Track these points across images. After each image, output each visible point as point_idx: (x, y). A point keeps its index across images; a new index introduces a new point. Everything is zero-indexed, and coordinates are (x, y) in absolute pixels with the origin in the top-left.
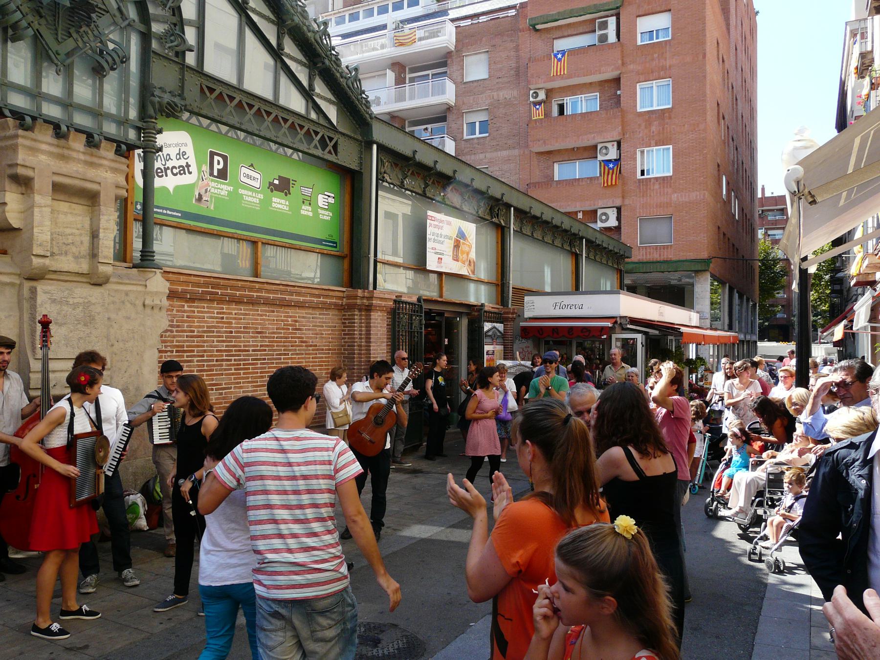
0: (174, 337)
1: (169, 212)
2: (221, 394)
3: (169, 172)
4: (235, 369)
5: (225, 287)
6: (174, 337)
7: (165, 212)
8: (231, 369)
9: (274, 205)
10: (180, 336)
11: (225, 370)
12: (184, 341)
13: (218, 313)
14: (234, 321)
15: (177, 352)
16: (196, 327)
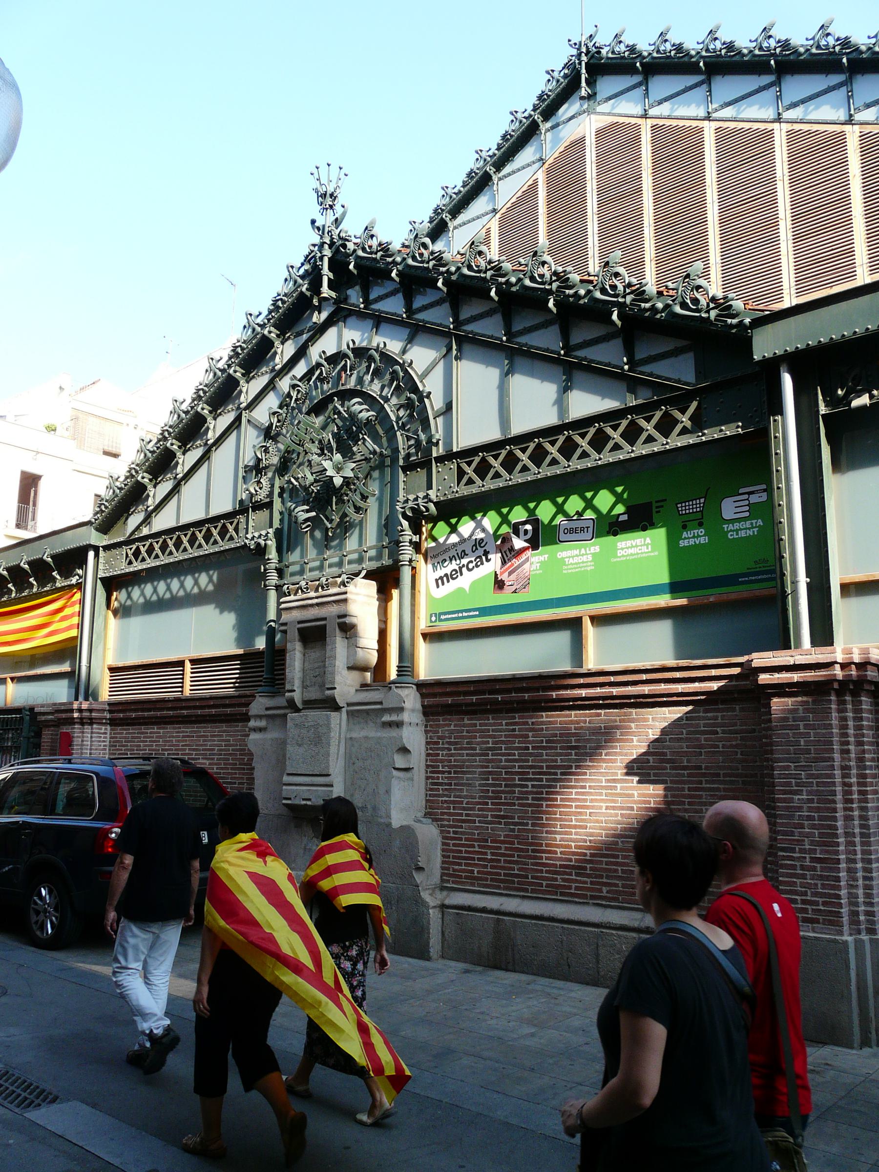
0: (452, 755)
1: (465, 614)
2: (513, 830)
3: (464, 570)
4: (533, 799)
5: (509, 691)
6: (452, 755)
7: (460, 615)
8: (527, 799)
9: (620, 553)
10: (460, 755)
11: (519, 798)
12: (464, 761)
13: (507, 724)
14: (530, 734)
15: (455, 772)
16: (478, 743)
